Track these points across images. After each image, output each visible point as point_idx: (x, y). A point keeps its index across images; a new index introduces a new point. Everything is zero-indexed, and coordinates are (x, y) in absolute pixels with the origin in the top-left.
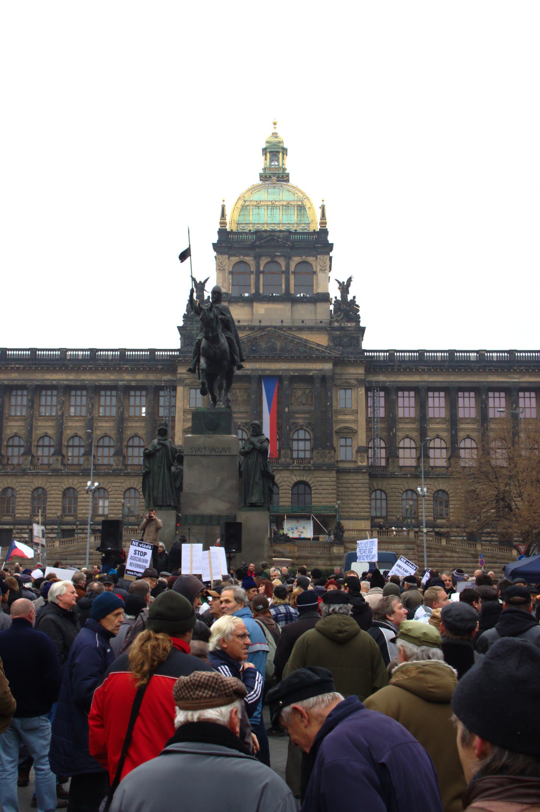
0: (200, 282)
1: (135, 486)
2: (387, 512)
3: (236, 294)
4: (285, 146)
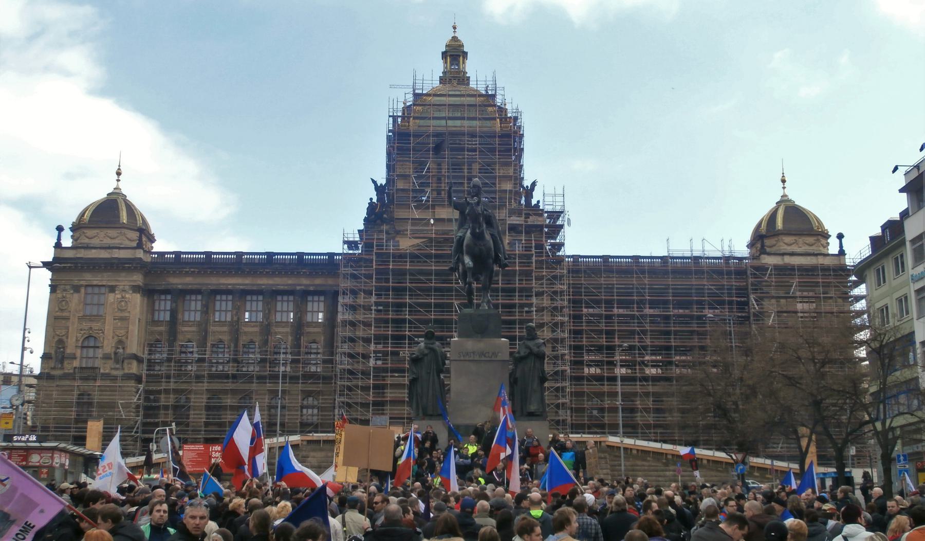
0: (381, 185)
4: (465, 50)
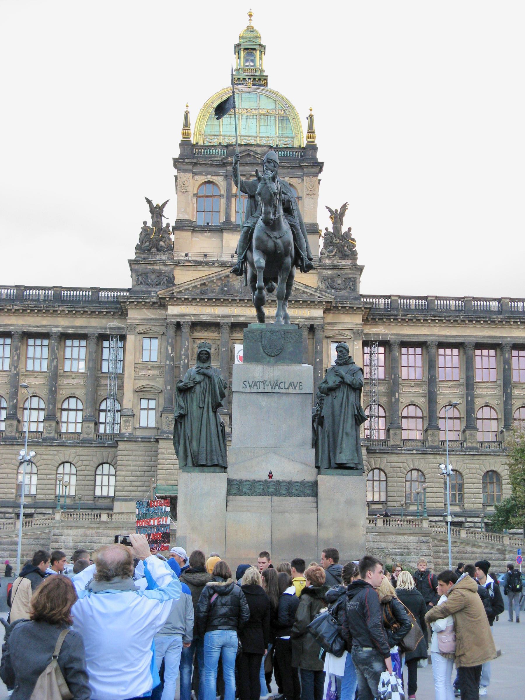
2: (387, 496)
3: (201, 222)
4: (263, 43)
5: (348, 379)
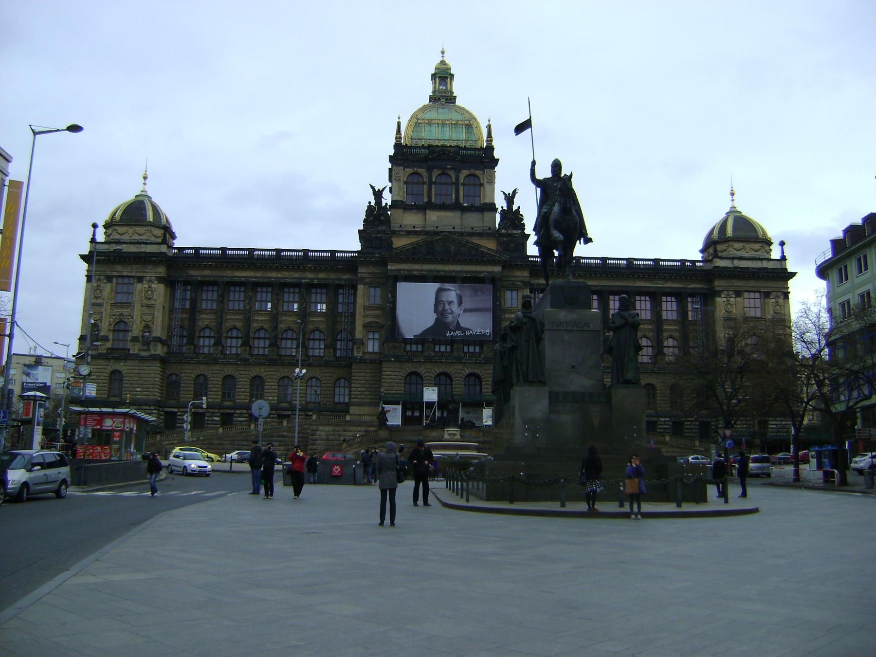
0: (379, 190)
1: (316, 376)
5: (631, 320)
